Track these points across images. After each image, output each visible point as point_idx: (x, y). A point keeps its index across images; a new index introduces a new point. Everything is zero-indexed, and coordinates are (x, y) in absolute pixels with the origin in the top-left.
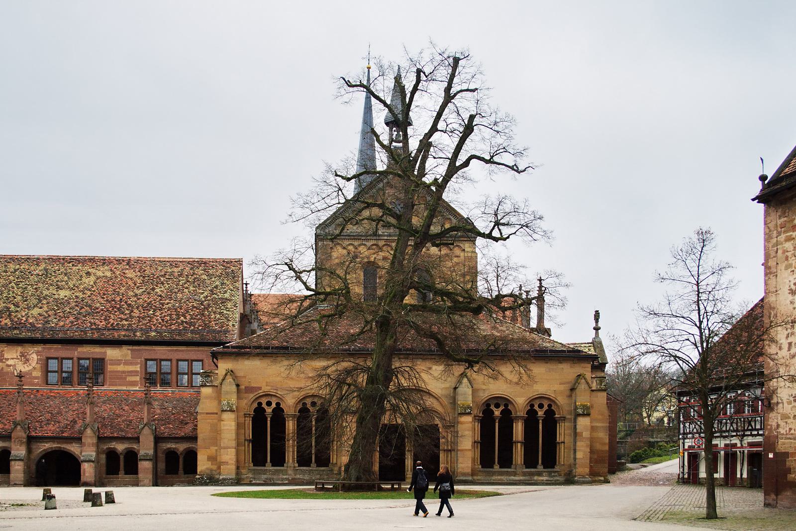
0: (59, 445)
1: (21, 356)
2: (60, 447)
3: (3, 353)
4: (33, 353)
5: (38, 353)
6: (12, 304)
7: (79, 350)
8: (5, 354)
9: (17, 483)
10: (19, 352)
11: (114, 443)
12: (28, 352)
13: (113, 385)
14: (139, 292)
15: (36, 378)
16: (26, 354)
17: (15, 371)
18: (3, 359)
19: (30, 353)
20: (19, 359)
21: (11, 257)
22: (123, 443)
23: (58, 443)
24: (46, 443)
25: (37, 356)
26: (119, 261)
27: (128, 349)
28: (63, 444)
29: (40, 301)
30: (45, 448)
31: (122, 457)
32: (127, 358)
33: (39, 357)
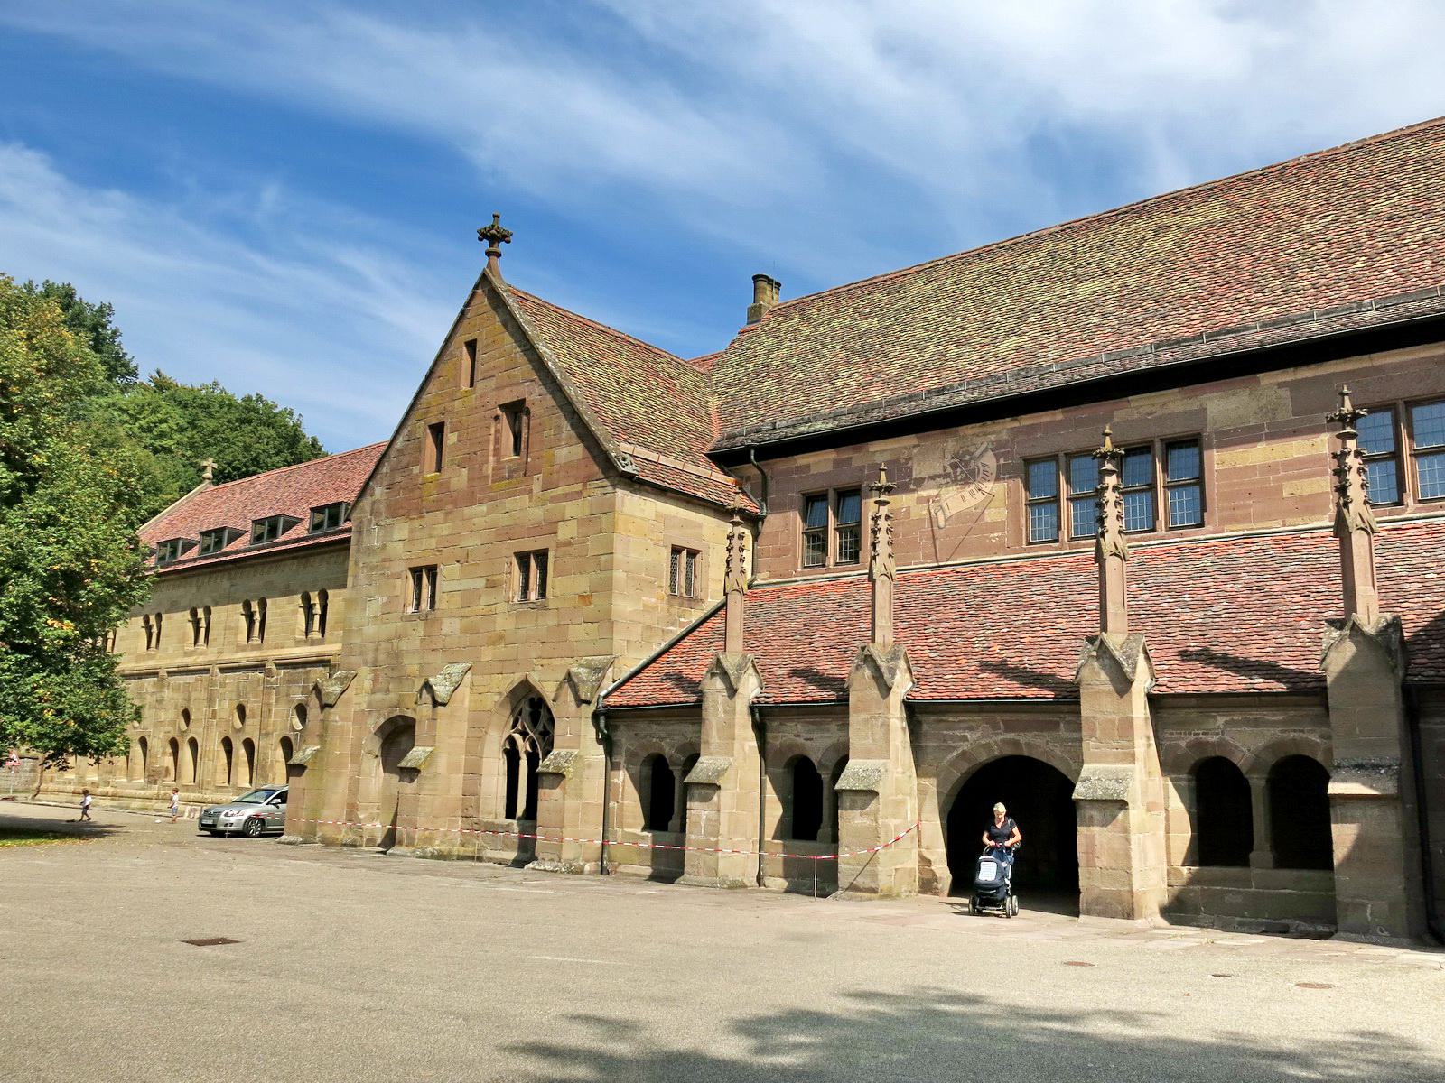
0: (1011, 736)
1: (951, 465)
2: (1016, 743)
3: (909, 465)
4: (986, 450)
5: (998, 449)
6: (955, 342)
7: (1115, 420)
8: (915, 467)
9: (860, 882)
10: (948, 456)
11: (1221, 720)
12: (971, 449)
13: (1235, 520)
14: (1308, 227)
15: (994, 527)
16: (967, 458)
17: (940, 513)
18: (909, 483)
19: (977, 454)
20: (948, 475)
21: (977, 252)
22: (1257, 723)
23: (1009, 727)
24: (971, 729)
25: (998, 461)
26: (1250, 179)
27: (1280, 385)
28: (1025, 730)
29: (1023, 317)
30: (965, 747)
31: (1257, 782)
32: (1280, 418)
33: (1002, 461)
